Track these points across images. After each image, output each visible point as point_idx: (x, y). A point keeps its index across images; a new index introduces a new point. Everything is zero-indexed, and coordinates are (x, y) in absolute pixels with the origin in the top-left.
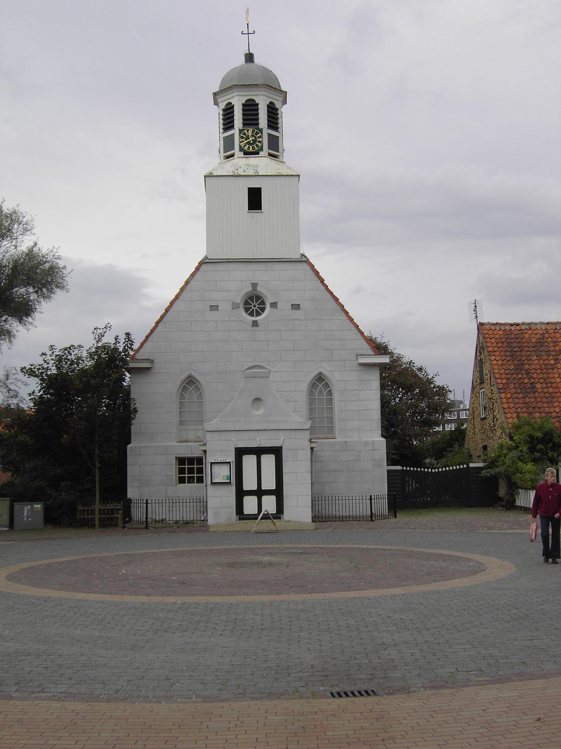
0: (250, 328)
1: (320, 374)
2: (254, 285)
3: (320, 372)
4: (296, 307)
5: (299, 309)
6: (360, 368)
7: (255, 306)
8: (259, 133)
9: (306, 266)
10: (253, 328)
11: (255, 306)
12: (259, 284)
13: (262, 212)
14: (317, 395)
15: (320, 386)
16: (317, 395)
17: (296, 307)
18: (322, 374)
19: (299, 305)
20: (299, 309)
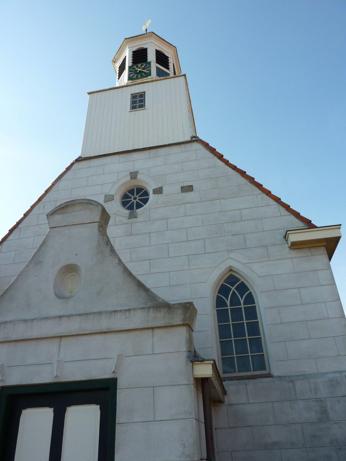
0: (125, 220)
1: (231, 270)
2: (134, 175)
3: (230, 266)
4: (187, 189)
5: (192, 190)
6: (294, 253)
7: (135, 199)
8: (147, 65)
9: (197, 146)
10: (130, 220)
11: (135, 199)
12: (139, 172)
13: (145, 109)
14: (228, 303)
15: (233, 288)
16: (228, 303)
17: (187, 189)
18: (233, 269)
19: (192, 186)
20: (192, 190)
